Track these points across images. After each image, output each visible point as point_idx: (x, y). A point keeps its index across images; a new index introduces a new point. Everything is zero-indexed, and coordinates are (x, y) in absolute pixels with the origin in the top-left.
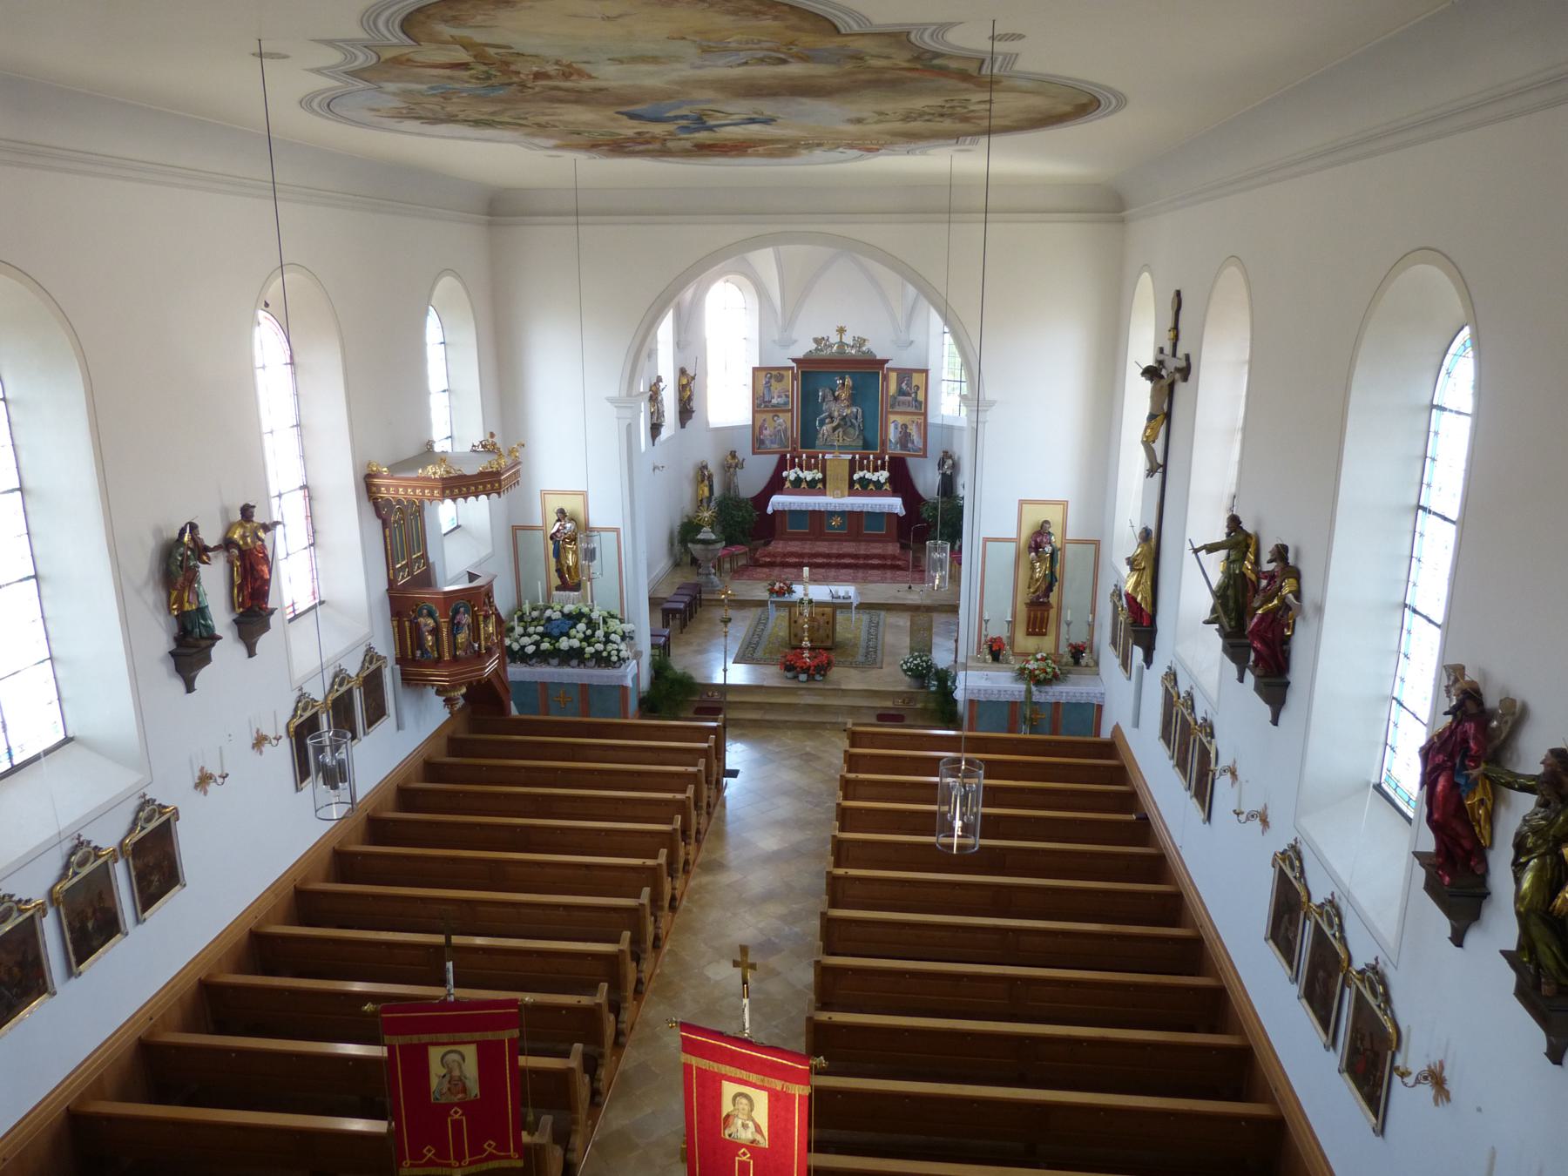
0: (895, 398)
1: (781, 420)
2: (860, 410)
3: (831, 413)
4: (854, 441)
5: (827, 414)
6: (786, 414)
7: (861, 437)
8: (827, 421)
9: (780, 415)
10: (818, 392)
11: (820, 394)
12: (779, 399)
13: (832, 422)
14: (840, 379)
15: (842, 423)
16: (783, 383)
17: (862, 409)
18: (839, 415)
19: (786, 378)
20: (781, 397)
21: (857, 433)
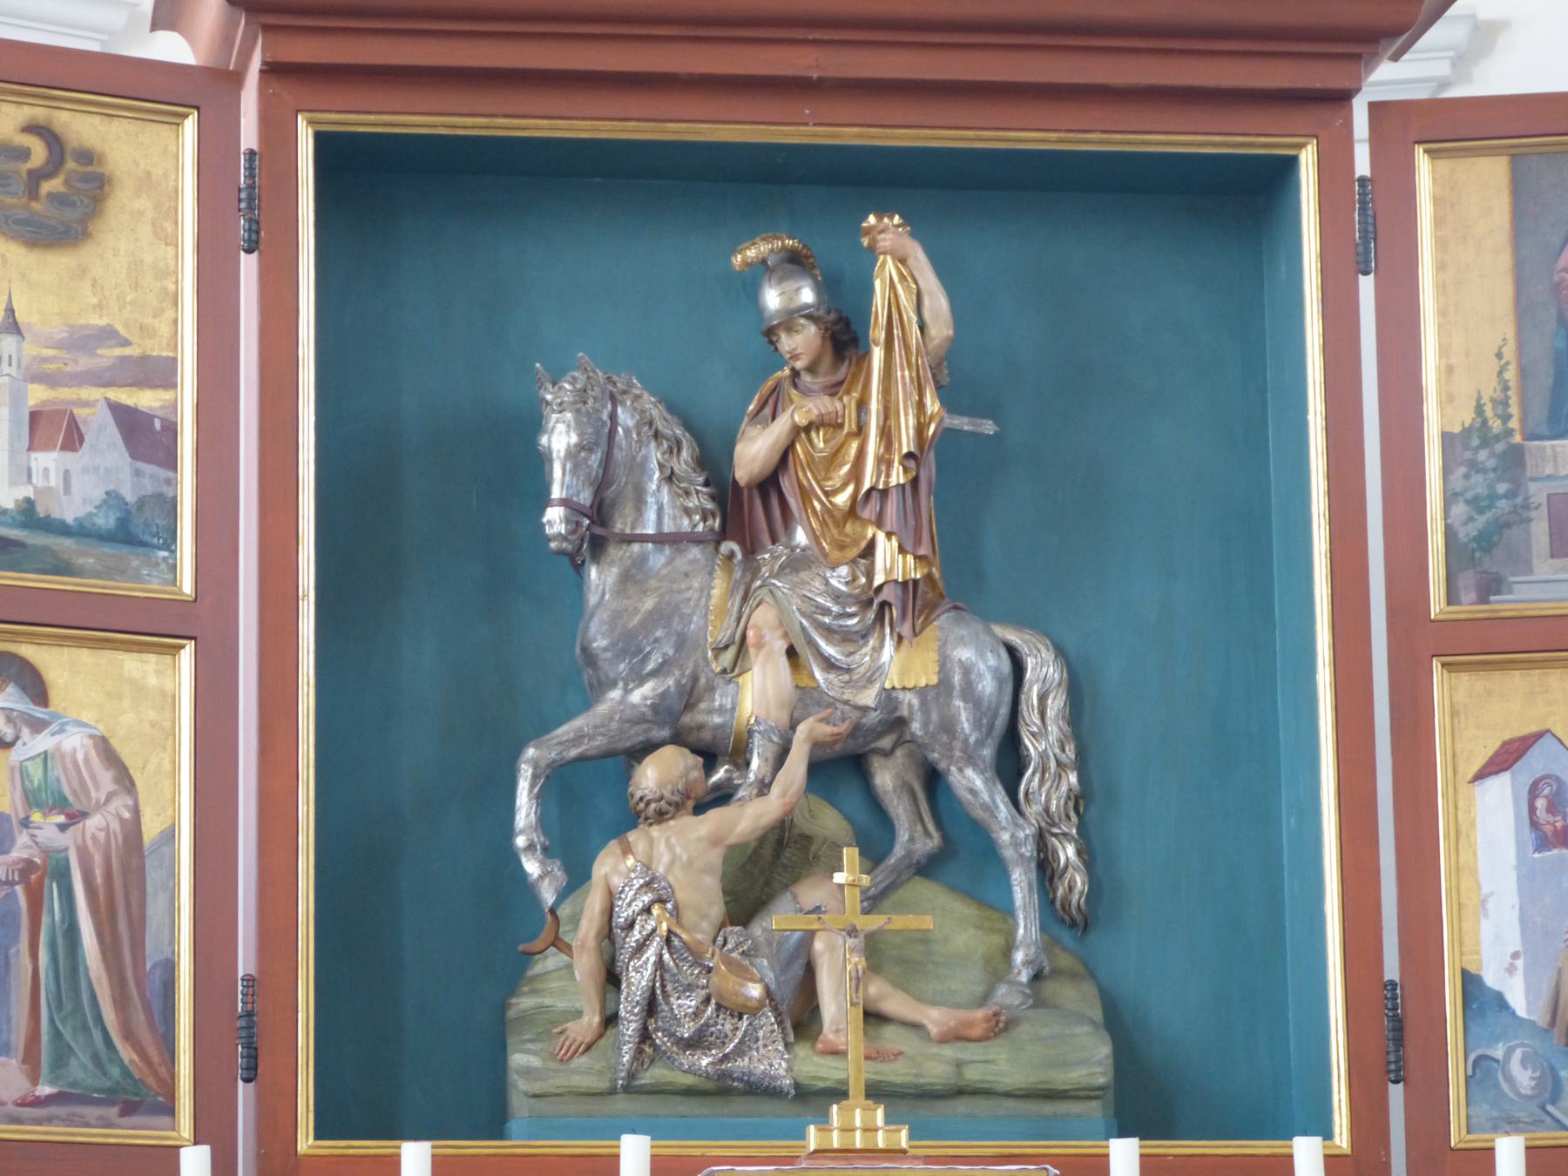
0: (1514, 460)
1: (74, 742)
2: (1043, 668)
3: (690, 695)
4: (1000, 1027)
5: (642, 694)
6: (140, 667)
7: (1077, 997)
8: (652, 776)
9: (54, 662)
10: (536, 425)
11: (559, 438)
12: (47, 462)
13: (722, 796)
14: (796, 262)
15: (828, 821)
16: (86, 254)
17: (1060, 652)
18: (806, 699)
19: (124, 204)
20: (73, 439)
21: (1026, 927)
